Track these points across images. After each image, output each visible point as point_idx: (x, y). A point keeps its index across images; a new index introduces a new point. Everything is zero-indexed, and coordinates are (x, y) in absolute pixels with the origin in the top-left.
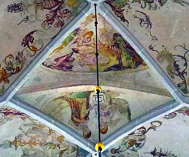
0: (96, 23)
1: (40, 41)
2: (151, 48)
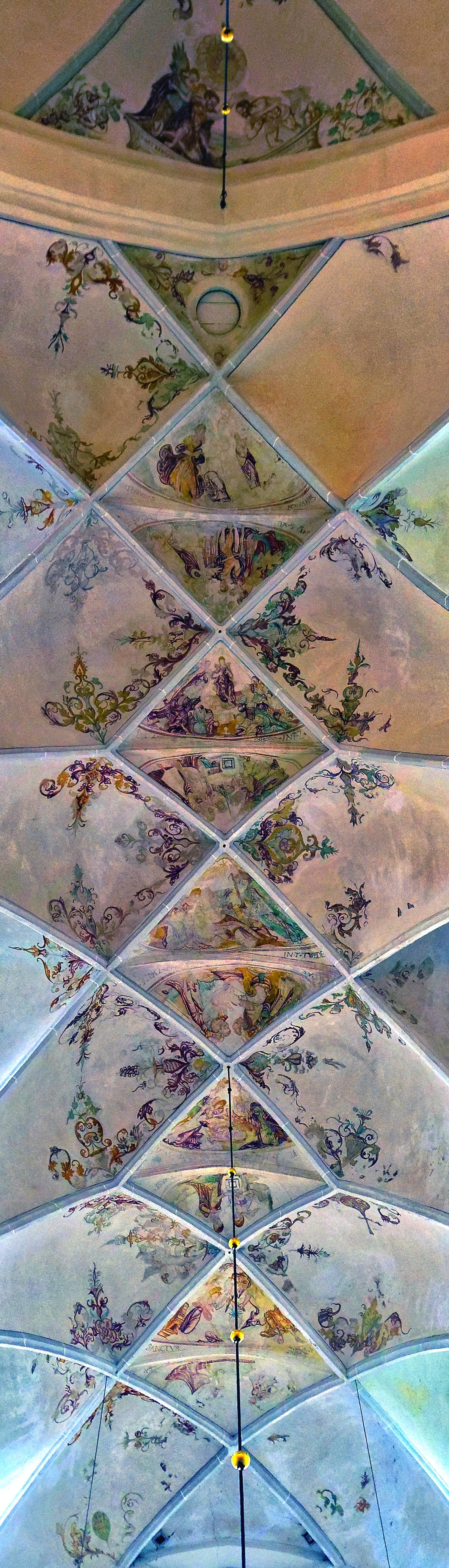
0: (230, 1090)
1: (160, 1112)
2: (297, 1121)
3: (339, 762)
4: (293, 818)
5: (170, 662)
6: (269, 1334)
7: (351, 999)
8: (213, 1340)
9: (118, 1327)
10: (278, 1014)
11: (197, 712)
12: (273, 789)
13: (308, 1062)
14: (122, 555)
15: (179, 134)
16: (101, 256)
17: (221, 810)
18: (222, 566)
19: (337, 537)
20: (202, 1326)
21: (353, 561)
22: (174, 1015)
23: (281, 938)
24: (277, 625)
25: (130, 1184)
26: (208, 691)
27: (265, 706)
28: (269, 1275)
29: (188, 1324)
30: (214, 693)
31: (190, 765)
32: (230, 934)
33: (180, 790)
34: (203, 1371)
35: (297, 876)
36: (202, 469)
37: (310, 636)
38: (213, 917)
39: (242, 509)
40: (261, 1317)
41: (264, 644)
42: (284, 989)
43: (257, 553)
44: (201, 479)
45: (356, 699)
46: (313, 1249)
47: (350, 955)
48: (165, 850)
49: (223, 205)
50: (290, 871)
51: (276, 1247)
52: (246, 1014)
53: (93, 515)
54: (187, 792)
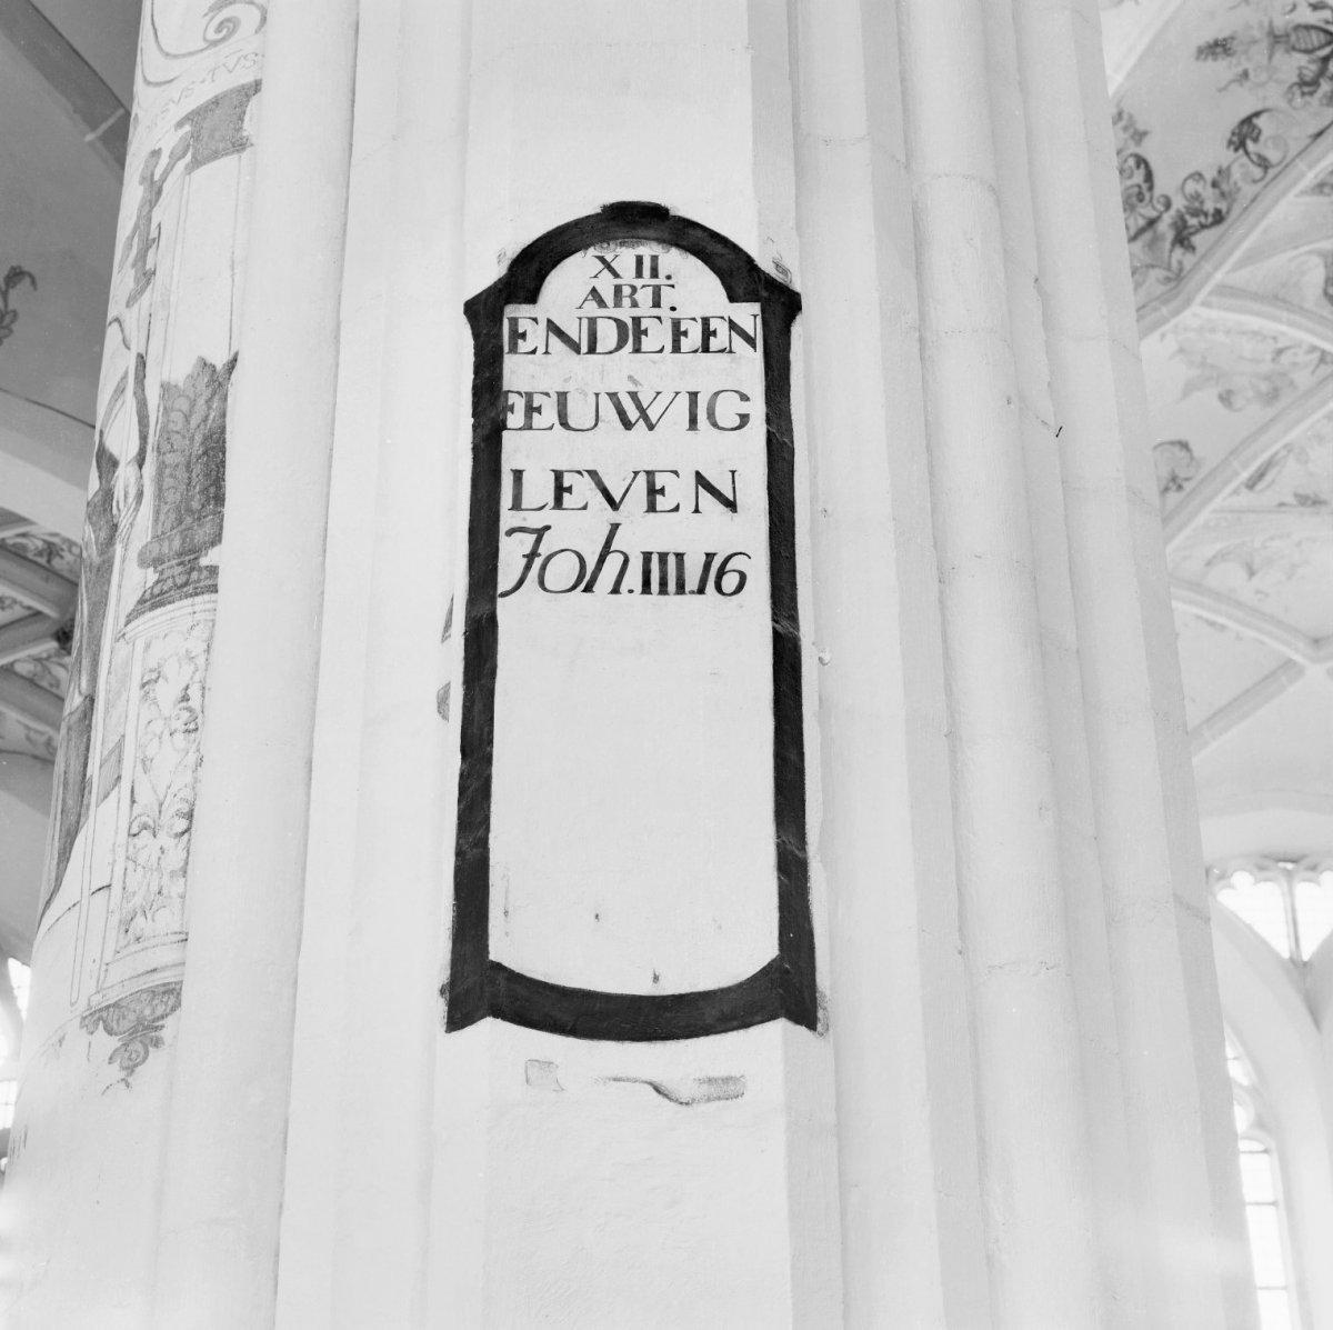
1: (1276, 139)
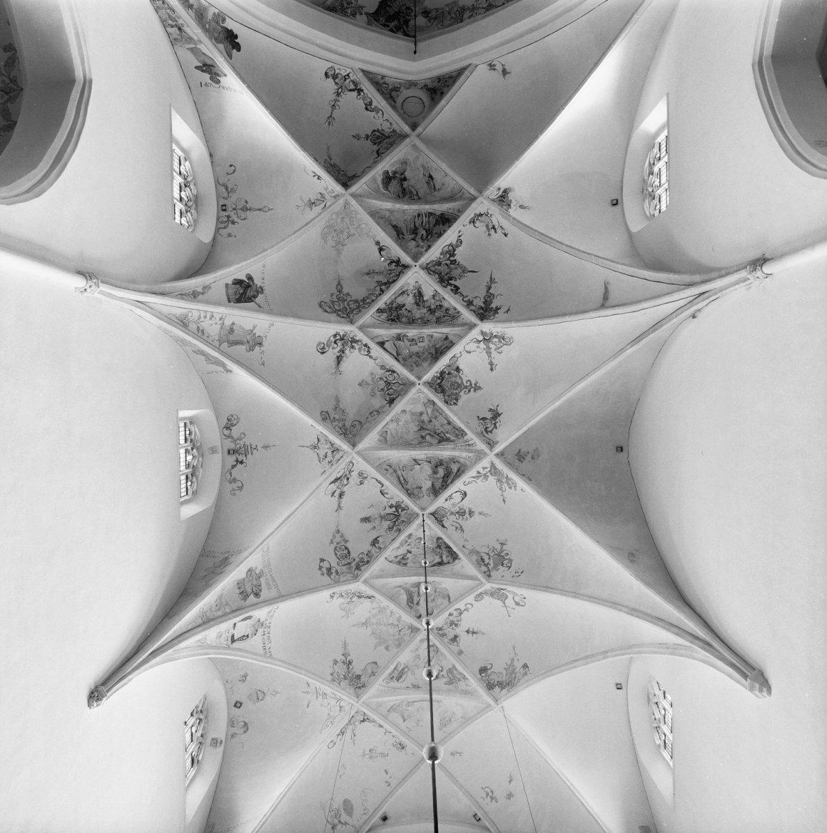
0: (424, 531)
1: (383, 543)
2: (464, 547)
3: (482, 333)
4: (458, 369)
5: (389, 284)
6: (450, 683)
7: (493, 470)
8: (416, 687)
9: (359, 677)
10: (452, 482)
11: (403, 311)
12: (446, 352)
13: (470, 514)
14: (363, 226)
15: (392, 25)
16: (352, 77)
17: (417, 366)
18: (417, 234)
19: (478, 213)
20: (409, 679)
21: (487, 226)
22: (392, 483)
23: (452, 438)
24: (446, 264)
25: (365, 582)
26: (409, 300)
27: (441, 306)
28: (449, 645)
29: (401, 677)
30: (413, 302)
31: (400, 340)
32: (423, 437)
33: (395, 354)
34: (410, 708)
35: (460, 403)
36: (405, 184)
37: (465, 270)
38: (414, 427)
39: (427, 203)
40: (444, 673)
41: (440, 274)
42: (454, 468)
43: (435, 226)
44: (404, 189)
45: (491, 300)
46: (475, 630)
47: (492, 443)
48: (386, 389)
49: (415, 52)
50: (457, 400)
51: (453, 629)
52: (433, 485)
53: (346, 204)
54: (398, 354)
